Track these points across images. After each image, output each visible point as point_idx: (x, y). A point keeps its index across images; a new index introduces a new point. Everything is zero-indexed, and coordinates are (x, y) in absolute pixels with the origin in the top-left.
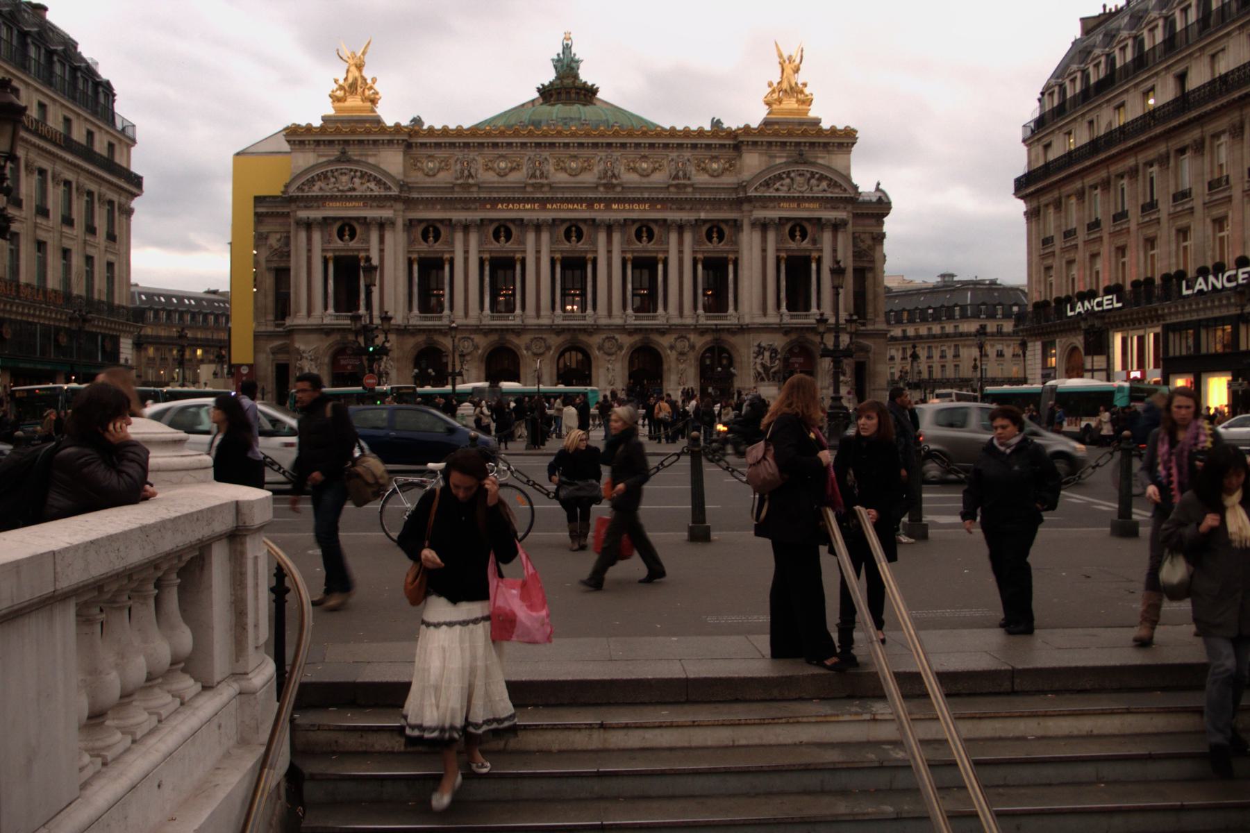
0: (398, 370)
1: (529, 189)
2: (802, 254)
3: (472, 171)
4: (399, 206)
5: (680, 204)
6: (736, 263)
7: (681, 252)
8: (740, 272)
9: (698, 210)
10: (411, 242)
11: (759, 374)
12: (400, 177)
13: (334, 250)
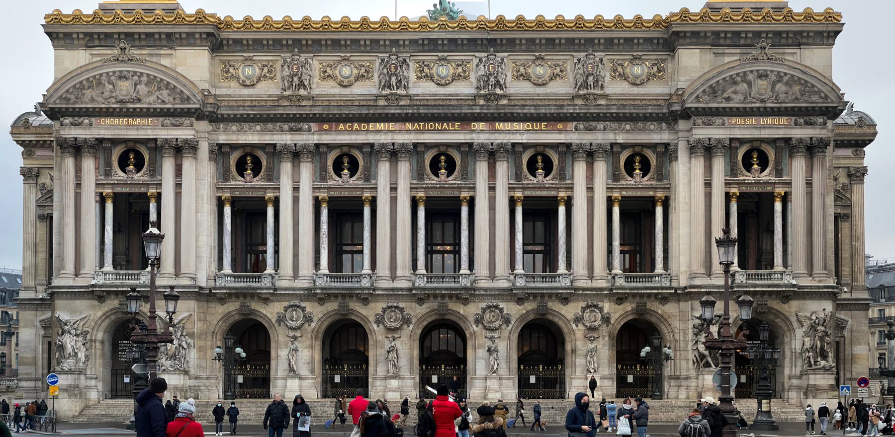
0: (200, 349)
1: (382, 102)
2: (760, 190)
3: (304, 77)
4: (203, 126)
6: (666, 203)
7: (590, 189)
8: (672, 217)
11: (702, 356)
12: (206, 86)
13: (113, 185)
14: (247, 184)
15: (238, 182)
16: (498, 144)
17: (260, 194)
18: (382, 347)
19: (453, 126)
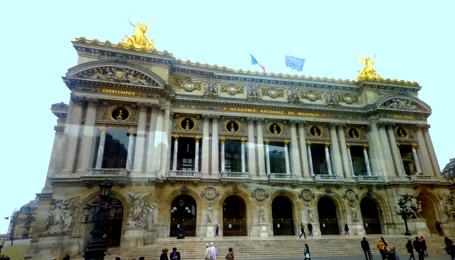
3: (215, 89)
5: (335, 114)
9: (346, 119)
10: (175, 127)
14: (187, 132)
15: (183, 130)
16: (300, 121)
17: (193, 136)
18: (255, 209)
19: (281, 112)
